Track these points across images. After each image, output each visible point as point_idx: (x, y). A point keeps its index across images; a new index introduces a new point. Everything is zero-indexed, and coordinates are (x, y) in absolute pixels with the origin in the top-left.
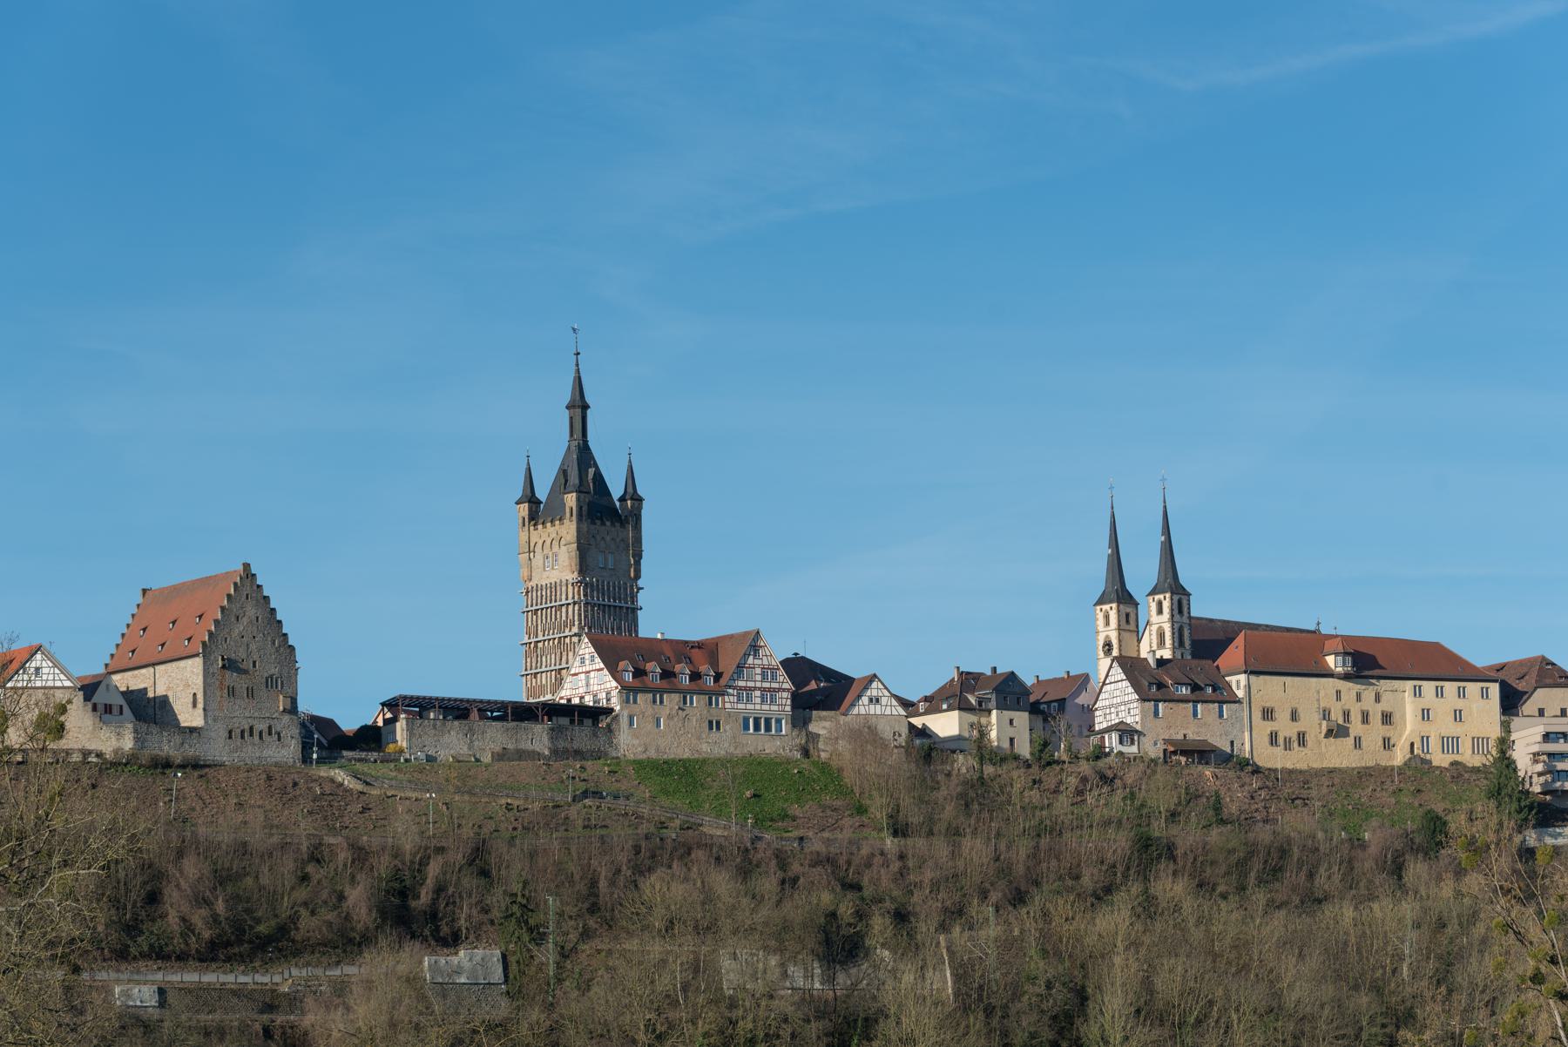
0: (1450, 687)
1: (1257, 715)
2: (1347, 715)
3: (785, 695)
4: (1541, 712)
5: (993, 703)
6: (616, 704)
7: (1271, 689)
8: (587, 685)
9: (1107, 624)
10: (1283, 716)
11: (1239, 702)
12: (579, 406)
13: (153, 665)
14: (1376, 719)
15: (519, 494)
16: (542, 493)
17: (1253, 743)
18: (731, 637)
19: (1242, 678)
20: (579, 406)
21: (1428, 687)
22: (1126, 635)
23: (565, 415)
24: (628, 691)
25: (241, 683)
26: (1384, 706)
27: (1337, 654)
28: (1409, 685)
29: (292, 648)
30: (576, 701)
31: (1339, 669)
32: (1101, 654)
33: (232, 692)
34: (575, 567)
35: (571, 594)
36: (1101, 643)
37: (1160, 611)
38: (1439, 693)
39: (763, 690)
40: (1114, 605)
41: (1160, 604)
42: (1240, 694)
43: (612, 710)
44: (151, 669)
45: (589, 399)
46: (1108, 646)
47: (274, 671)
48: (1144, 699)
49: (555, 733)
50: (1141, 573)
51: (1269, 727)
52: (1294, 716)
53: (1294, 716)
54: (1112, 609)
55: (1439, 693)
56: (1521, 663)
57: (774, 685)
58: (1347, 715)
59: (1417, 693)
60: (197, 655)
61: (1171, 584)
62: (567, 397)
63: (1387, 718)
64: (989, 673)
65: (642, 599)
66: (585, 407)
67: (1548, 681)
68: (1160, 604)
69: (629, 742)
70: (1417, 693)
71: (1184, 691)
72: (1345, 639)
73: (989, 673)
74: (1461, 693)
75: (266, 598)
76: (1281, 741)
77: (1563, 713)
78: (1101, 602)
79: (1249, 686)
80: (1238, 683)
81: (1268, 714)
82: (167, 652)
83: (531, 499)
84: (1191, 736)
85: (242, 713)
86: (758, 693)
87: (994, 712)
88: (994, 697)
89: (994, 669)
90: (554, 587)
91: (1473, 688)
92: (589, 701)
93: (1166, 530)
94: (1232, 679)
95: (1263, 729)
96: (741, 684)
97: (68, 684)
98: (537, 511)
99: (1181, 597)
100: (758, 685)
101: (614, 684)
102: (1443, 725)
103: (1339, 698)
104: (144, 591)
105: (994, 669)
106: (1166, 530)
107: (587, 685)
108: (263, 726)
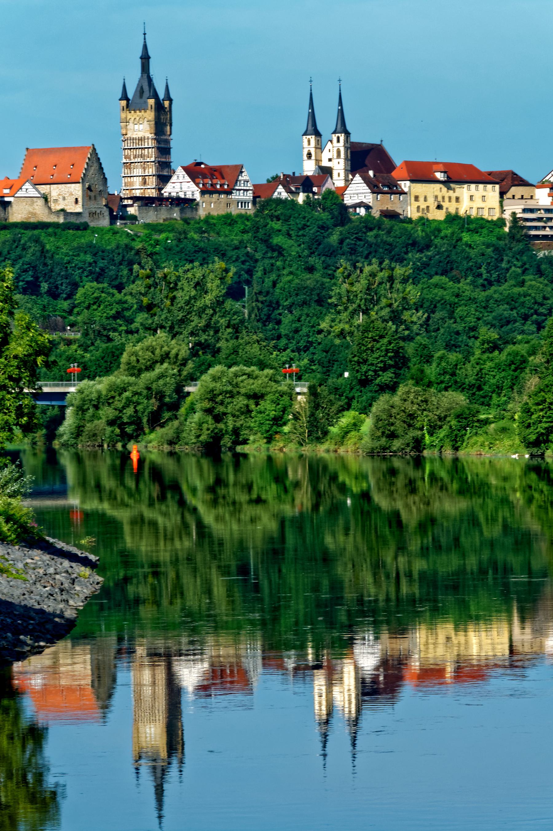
0: (481, 186)
1: (413, 199)
2: (443, 198)
3: (251, 192)
4: (514, 196)
5: (301, 190)
6: (197, 196)
7: (420, 189)
8: (181, 188)
9: (309, 144)
10: (421, 199)
11: (406, 193)
12: (145, 58)
13: (50, 184)
14: (454, 200)
15: (120, 96)
16: (130, 95)
17: (412, 212)
18: (228, 166)
19: (408, 183)
20: (145, 58)
21: (473, 186)
22: (318, 150)
23: (139, 62)
24: (203, 192)
25: (92, 194)
26: (457, 194)
27: (441, 172)
28: (466, 186)
29: (106, 179)
30: (174, 194)
31: (442, 179)
32: (305, 157)
33: (90, 198)
34: (153, 131)
35: (151, 143)
36: (305, 152)
37: (338, 141)
38: (477, 189)
39: (244, 190)
40: (313, 136)
41: (338, 138)
42: (406, 190)
43: (195, 200)
44: (48, 186)
45: (150, 53)
46: (309, 155)
47: (101, 188)
48: (373, 192)
49: (182, 211)
50: (327, 121)
51: (417, 204)
52: (425, 200)
53: (425, 200)
54: (313, 139)
55: (477, 189)
56: (501, 173)
57: (248, 188)
58: (443, 198)
59: (469, 189)
60: (79, 183)
61: (342, 127)
62: (140, 54)
63: (457, 199)
64: (292, 174)
65: (172, 144)
66: (149, 58)
67: (516, 183)
68: (338, 138)
69: (202, 213)
70: (469, 189)
71: (386, 189)
72: (445, 164)
73: (292, 174)
74: (485, 190)
75: (99, 159)
76: (421, 210)
77: (522, 197)
78: (305, 134)
79: (410, 187)
80: (405, 185)
81: (417, 198)
82: (55, 178)
83: (125, 97)
84: (390, 208)
85: (93, 206)
86: (242, 191)
87: (301, 194)
88: (301, 187)
89: (294, 173)
90: (141, 139)
91: (489, 186)
92: (182, 195)
93: (340, 103)
94: (402, 183)
95: (415, 204)
96: (237, 188)
97: (39, 196)
98: (130, 104)
99: (348, 134)
100: (243, 188)
101: (197, 188)
102: (478, 203)
103: (441, 191)
104: (27, 149)
105: (294, 173)
106: (340, 103)
107: (181, 188)
108: (98, 211)
